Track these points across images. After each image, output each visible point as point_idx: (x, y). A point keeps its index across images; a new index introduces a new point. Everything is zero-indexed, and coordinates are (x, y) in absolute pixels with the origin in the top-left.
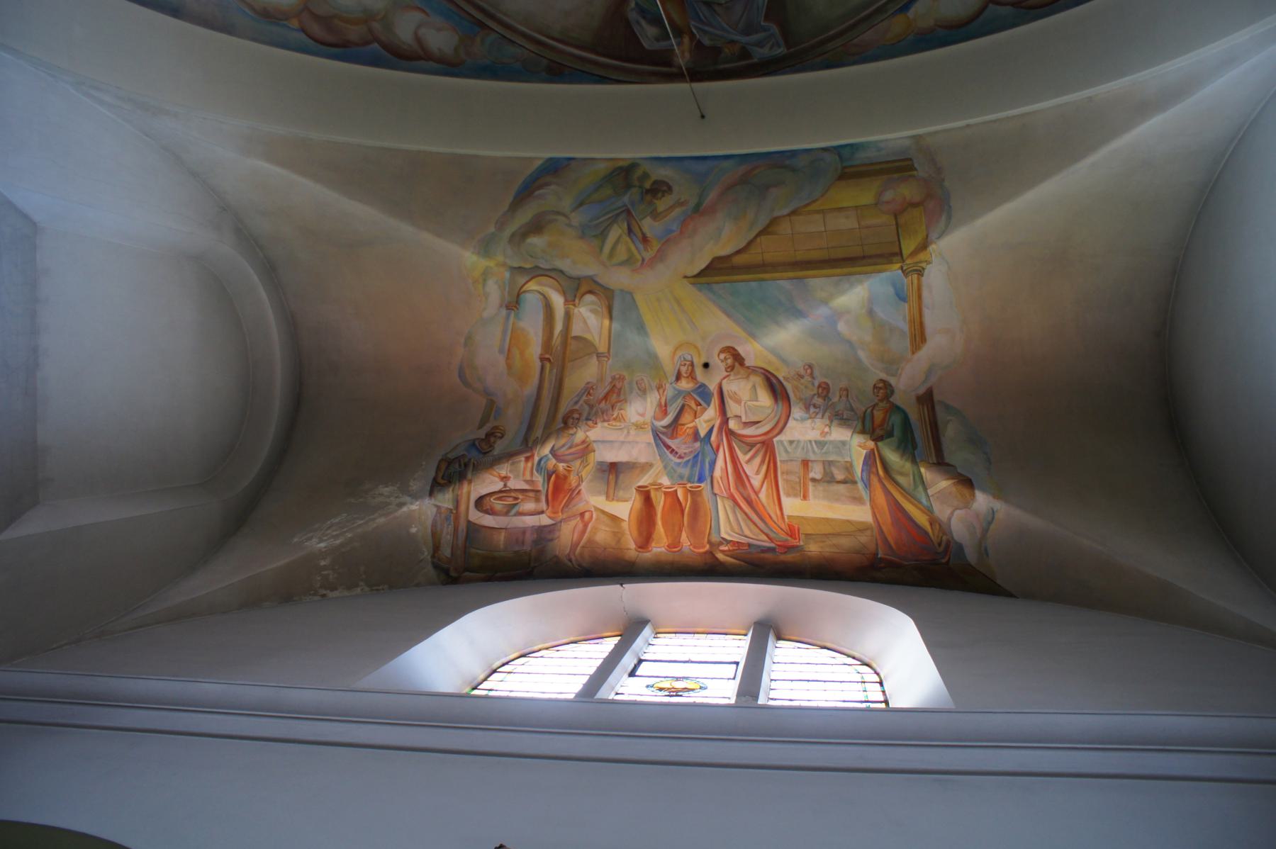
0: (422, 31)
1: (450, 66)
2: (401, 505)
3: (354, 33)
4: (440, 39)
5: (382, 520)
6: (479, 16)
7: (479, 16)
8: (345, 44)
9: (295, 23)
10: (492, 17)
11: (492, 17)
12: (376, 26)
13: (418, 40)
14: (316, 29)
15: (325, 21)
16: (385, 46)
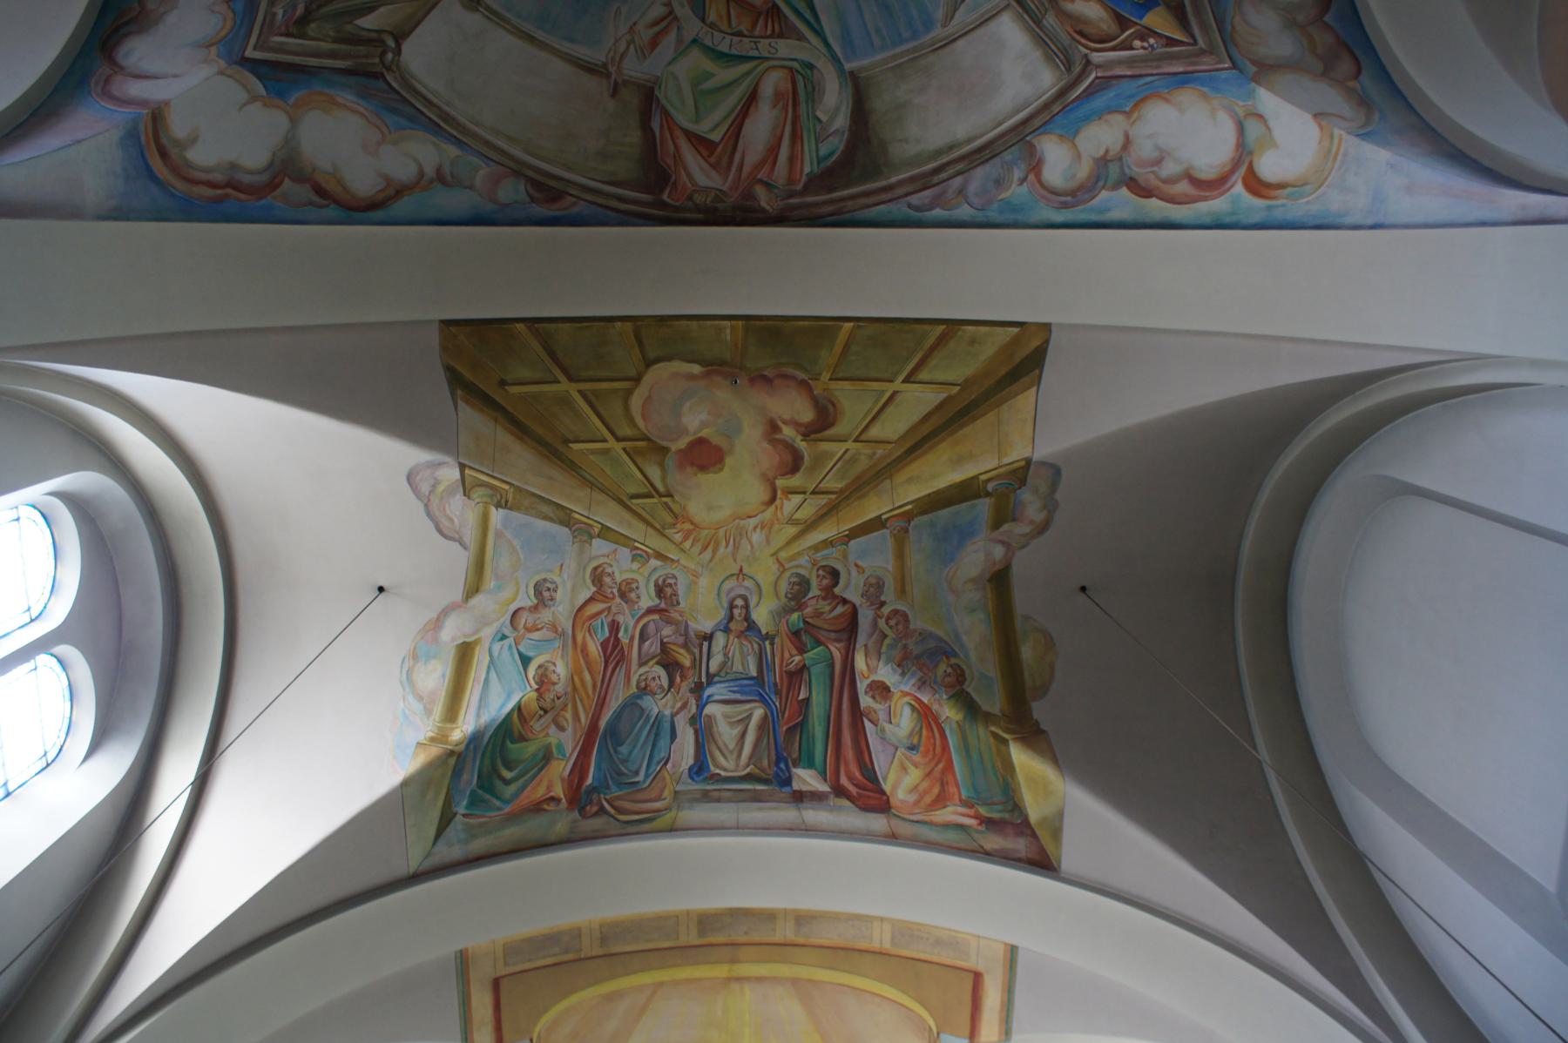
14: (1345, 66)
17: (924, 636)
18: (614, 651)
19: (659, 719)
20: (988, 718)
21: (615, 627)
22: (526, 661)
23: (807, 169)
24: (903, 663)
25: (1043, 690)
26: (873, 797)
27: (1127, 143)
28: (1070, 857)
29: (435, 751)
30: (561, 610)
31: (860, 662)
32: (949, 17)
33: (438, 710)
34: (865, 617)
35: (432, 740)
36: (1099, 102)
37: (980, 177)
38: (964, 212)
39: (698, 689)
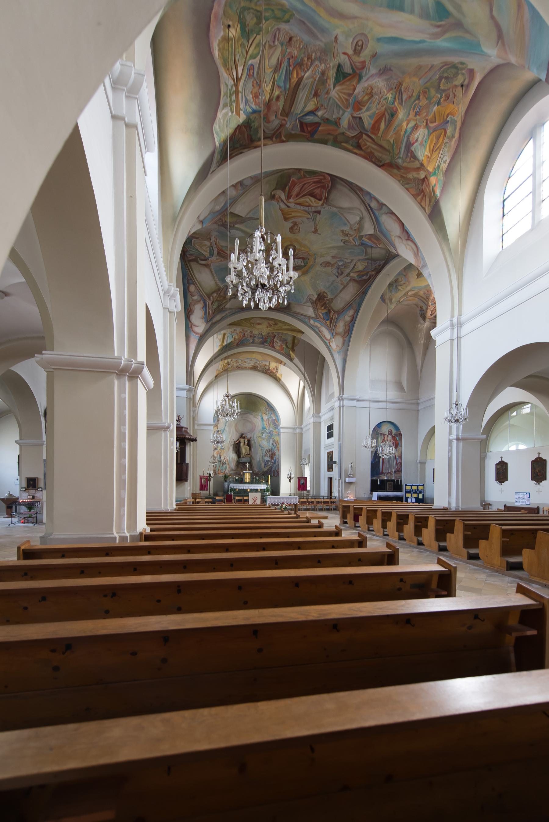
0: (349, 316)
1: (357, 311)
2: (424, 327)
3: (347, 328)
4: (351, 312)
5: (424, 331)
6: (349, 305)
7: (349, 305)
8: (349, 330)
9: (345, 339)
10: (350, 303)
11: (350, 303)
12: (346, 324)
13: (351, 316)
14: (346, 335)
15: (345, 333)
16: (350, 323)
17: (284, 338)
18: (244, 336)
19: (248, 340)
20: (289, 348)
21: (244, 334)
22: (232, 336)
23: (280, 307)
24: (280, 341)
25: (296, 346)
26: (273, 347)
27: (320, 327)
28: (294, 361)
29: (221, 346)
30: (238, 332)
31: (275, 339)
32: (304, 303)
33: (221, 341)
34: (277, 336)
35: (221, 345)
36: (319, 322)
37: (302, 317)
38: (299, 318)
39: (254, 338)
